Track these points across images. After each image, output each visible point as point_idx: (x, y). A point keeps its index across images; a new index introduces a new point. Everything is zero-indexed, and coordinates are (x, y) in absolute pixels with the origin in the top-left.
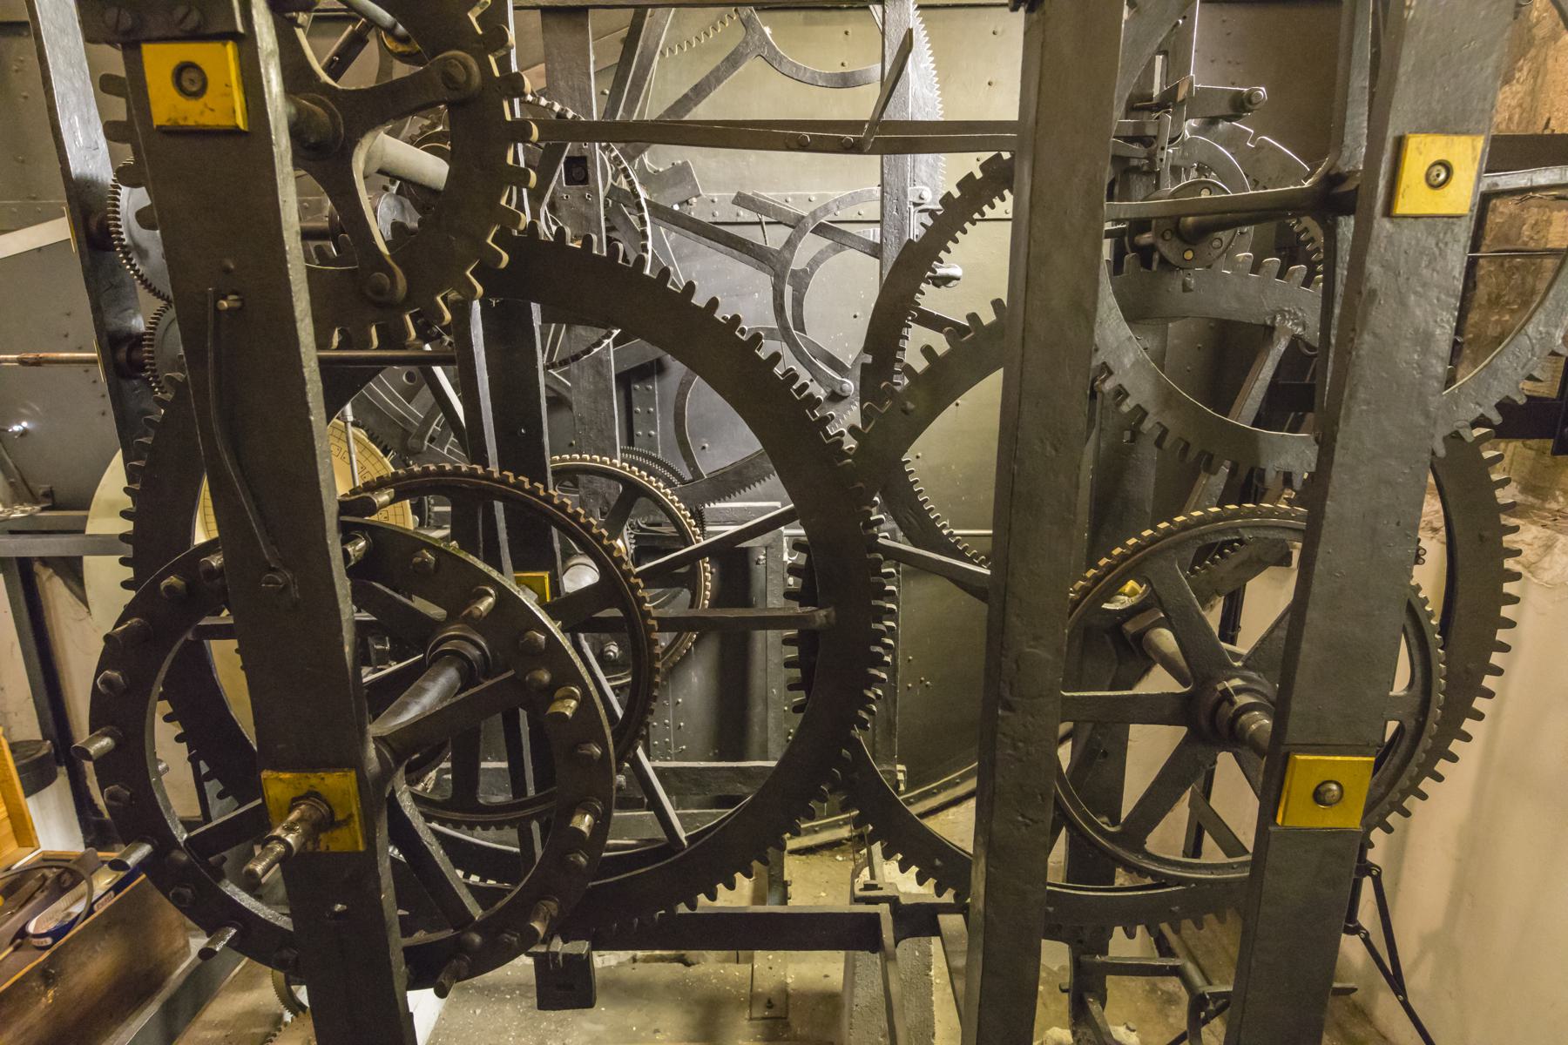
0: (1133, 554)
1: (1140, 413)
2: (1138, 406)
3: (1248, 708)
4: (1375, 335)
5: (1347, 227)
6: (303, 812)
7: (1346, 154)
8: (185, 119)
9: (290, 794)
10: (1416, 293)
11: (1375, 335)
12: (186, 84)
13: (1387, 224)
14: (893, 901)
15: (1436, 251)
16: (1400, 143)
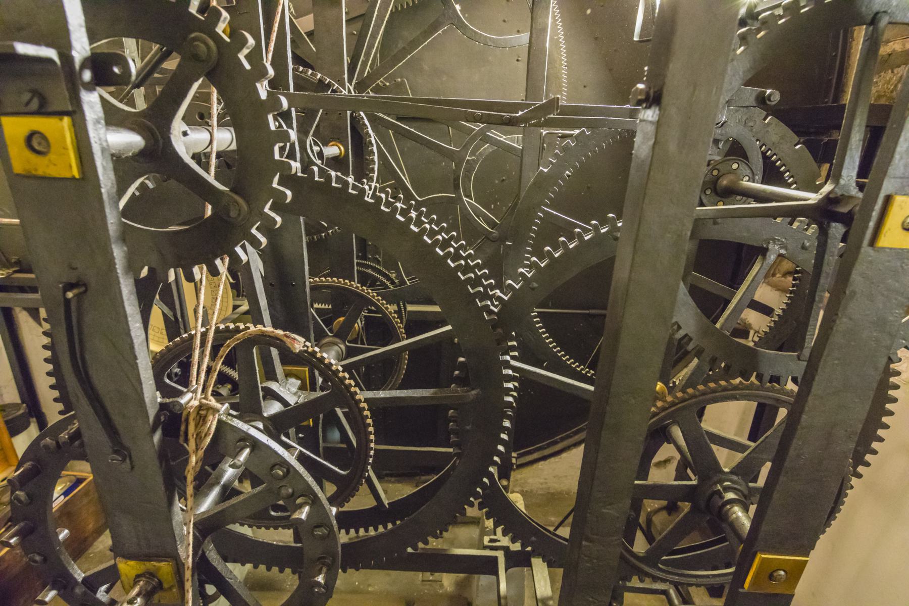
0: (670, 407)
1: (687, 338)
2: (686, 335)
3: (731, 502)
4: (851, 319)
5: (837, 230)
6: (141, 588)
7: (842, 182)
8: (36, 170)
9: (133, 573)
10: (883, 295)
11: (851, 319)
12: (37, 148)
13: (870, 250)
14: (506, 549)
15: (900, 270)
16: (888, 199)
